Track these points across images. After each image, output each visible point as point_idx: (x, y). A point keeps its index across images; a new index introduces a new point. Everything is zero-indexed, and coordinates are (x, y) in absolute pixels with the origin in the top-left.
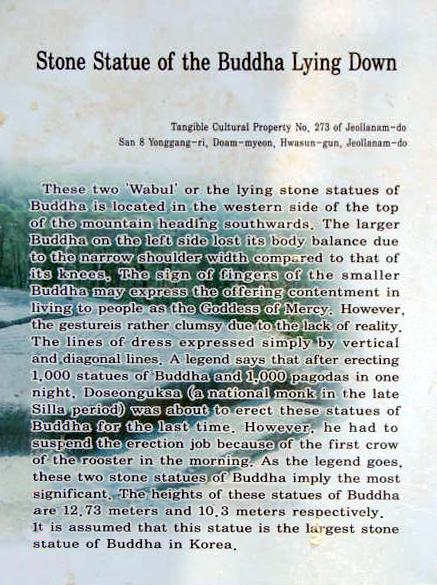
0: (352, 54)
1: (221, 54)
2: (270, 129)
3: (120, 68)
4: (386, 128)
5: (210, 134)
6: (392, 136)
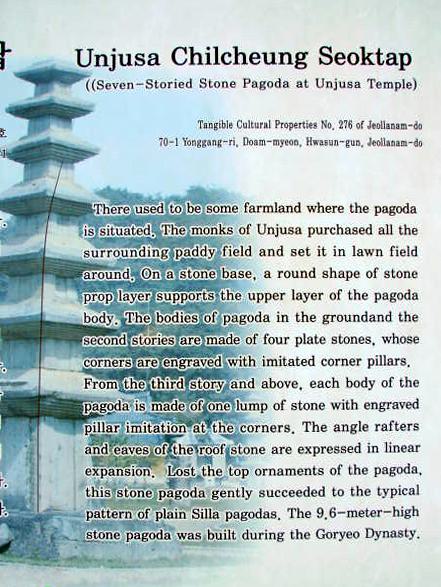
4: (404, 126)
6: (408, 135)
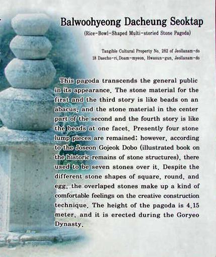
0: (126, 18)
1: (62, 18)
2: (143, 52)
3: (70, 25)
5: (118, 55)
